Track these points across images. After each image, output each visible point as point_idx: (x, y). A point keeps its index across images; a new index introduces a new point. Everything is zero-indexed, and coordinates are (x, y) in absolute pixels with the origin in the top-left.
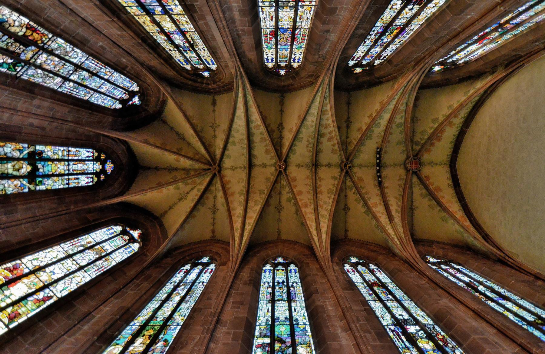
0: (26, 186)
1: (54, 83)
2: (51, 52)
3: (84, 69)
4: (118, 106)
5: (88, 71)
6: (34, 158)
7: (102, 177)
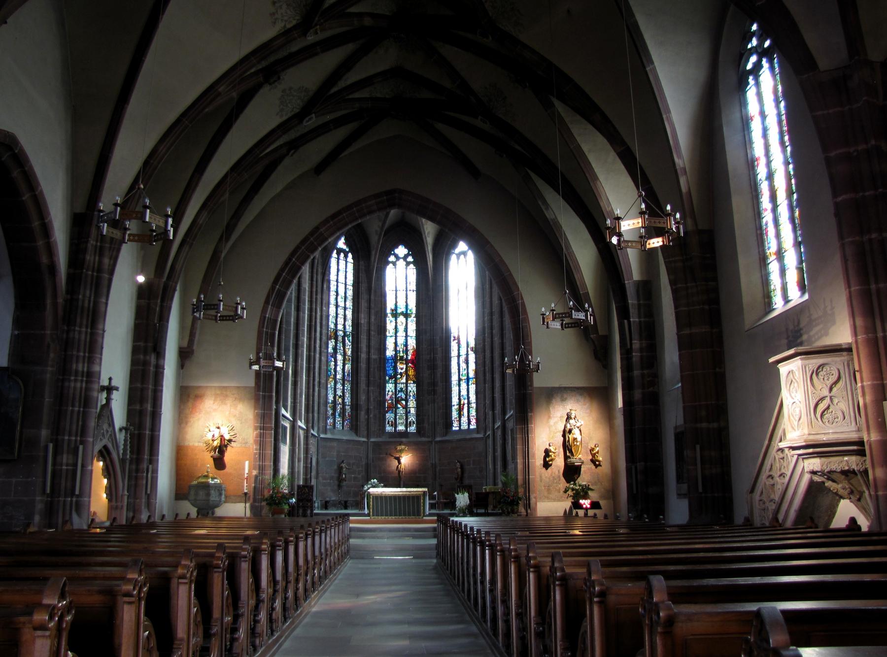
1: (349, 314)
2: (336, 325)
3: (337, 302)
4: (350, 255)
5: (336, 299)
6: (395, 315)
7: (410, 259)
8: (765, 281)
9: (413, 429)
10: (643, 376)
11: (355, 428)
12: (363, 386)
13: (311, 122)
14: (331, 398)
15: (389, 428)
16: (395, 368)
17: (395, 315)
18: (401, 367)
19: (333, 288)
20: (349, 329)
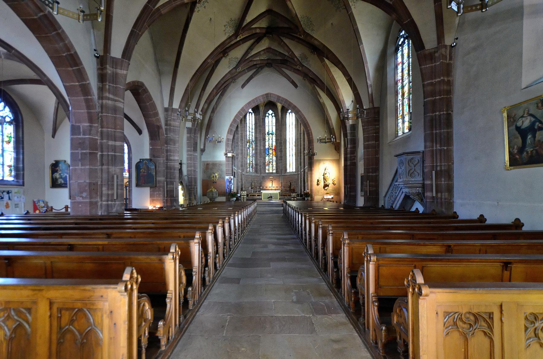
0: (274, 135)
1: (254, 134)
6: (268, 134)
7: (273, 115)
8: (397, 125)
9: (274, 171)
10: (351, 157)
11: (256, 171)
12: (258, 158)
13: (240, 69)
14: (248, 162)
15: (267, 171)
16: (269, 152)
17: (268, 134)
18: (271, 151)
19: (248, 125)
20: (254, 139)
